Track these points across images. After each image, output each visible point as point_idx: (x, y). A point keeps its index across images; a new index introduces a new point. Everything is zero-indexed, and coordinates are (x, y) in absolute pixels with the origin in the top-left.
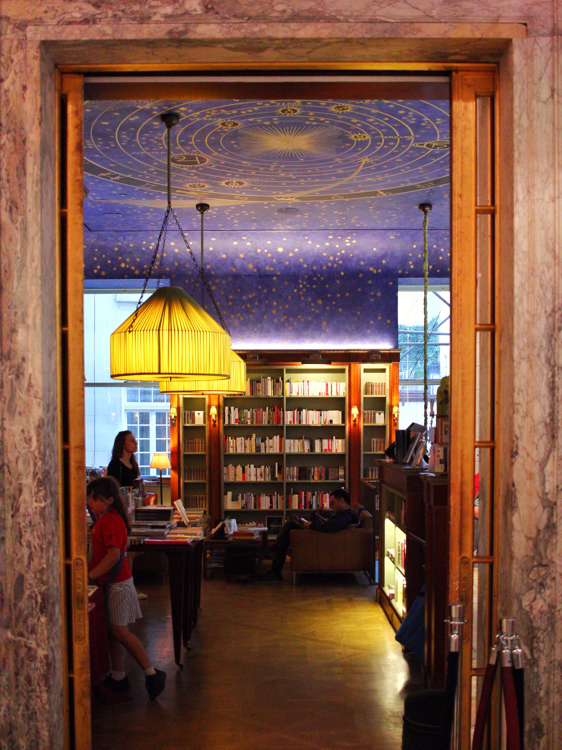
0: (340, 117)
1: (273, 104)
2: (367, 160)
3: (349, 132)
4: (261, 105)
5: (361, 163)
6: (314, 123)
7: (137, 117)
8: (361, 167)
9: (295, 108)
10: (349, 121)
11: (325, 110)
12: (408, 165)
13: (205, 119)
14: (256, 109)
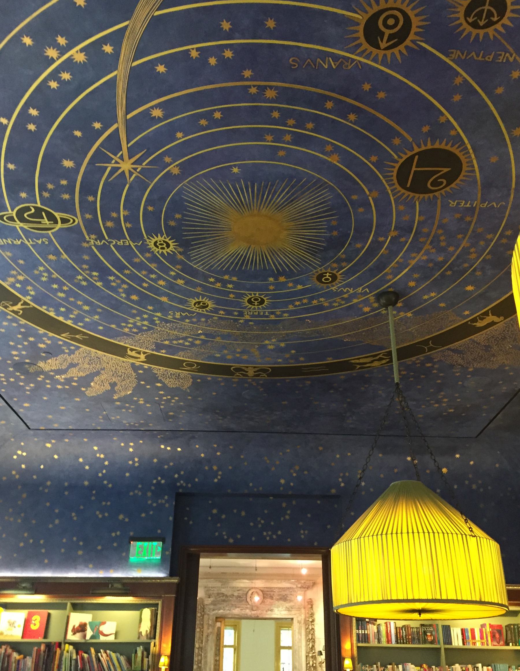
0: (198, 290)
1: (272, 313)
2: (126, 166)
4: (284, 312)
5: (131, 153)
6: (226, 277)
7: (426, 297)
8: (120, 125)
9: (250, 306)
11: (218, 302)
12: (39, 136)
13: (351, 291)
14: (291, 307)
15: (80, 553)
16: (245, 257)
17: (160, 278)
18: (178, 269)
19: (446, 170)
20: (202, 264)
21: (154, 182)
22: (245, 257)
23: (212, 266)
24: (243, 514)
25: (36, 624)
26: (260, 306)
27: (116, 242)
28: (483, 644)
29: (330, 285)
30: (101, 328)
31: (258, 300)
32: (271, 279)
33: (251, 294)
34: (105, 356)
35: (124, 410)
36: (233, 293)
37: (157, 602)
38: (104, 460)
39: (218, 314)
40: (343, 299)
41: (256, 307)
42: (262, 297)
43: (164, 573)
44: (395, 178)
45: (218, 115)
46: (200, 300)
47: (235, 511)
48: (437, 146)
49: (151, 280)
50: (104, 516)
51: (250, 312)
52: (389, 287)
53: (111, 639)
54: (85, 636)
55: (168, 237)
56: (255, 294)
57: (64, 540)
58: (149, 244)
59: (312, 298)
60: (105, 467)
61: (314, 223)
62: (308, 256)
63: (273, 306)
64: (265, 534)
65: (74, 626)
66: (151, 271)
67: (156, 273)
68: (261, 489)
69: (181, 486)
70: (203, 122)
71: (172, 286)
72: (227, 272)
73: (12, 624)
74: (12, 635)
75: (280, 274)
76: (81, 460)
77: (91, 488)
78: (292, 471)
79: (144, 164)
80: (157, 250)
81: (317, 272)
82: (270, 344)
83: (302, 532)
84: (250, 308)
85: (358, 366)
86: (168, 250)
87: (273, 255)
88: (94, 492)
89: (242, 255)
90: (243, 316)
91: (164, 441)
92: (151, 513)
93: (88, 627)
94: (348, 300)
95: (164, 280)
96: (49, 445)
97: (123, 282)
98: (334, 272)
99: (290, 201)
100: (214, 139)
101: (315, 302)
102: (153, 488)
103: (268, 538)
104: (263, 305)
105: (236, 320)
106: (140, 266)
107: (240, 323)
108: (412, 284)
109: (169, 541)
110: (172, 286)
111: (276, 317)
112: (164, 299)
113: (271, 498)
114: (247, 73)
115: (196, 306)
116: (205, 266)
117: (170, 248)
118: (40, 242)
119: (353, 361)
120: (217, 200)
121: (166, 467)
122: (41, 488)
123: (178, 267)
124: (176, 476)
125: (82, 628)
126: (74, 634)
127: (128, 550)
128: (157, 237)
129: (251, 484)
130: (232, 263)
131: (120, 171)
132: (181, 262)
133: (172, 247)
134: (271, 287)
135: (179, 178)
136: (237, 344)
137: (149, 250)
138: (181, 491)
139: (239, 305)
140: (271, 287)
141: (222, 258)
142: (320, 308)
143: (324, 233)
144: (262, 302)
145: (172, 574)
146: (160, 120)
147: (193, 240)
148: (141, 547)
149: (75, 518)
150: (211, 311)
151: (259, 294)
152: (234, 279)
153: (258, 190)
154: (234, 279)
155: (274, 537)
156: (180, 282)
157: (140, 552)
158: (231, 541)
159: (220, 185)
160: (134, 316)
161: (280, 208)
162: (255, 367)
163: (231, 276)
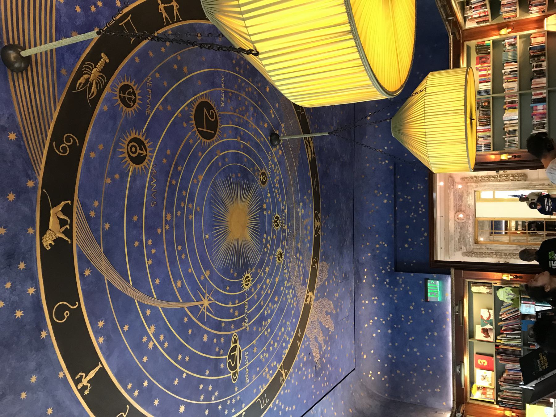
0: (271, 258)
1: (283, 211)
2: (206, 303)
3: (253, 270)
4: (283, 204)
6: (264, 241)
7: (273, 116)
8: (185, 306)
9: (280, 225)
10: (267, 265)
11: (278, 246)
12: (192, 355)
13: (270, 163)
14: (280, 200)
15: (436, 334)
16: (253, 229)
17: (265, 282)
18: (260, 271)
19: (205, 110)
20: (257, 256)
21: (214, 286)
22: (253, 229)
23: (258, 250)
24: (408, 227)
25: (483, 362)
26: (280, 219)
27: (246, 310)
28: (489, 70)
29: (267, 176)
30: (294, 320)
31: (276, 221)
32: (265, 213)
33: (273, 225)
34: (310, 318)
35: (342, 307)
36: (273, 236)
37: (467, 282)
38: (374, 320)
39: (284, 246)
40: (275, 168)
41: (280, 221)
42: (274, 218)
43: (448, 279)
44: (210, 141)
45: (180, 248)
46: (277, 257)
47: (406, 232)
48: (193, 117)
49: (266, 288)
50: (411, 319)
51: (283, 225)
52: (268, 139)
53: (492, 312)
54: (491, 329)
55: (243, 277)
56: (273, 223)
57: (428, 344)
58: (247, 289)
59: (275, 187)
60: (378, 319)
61: (234, 188)
62: (252, 190)
63: (279, 211)
64: (421, 212)
65: (484, 337)
66: (262, 288)
67: (262, 285)
68: (391, 215)
69: (390, 268)
70: (183, 256)
71: (270, 275)
72: (261, 241)
73: (484, 378)
74: (492, 378)
75: (262, 208)
76: (374, 335)
77: (392, 328)
78: (378, 195)
79: (205, 292)
80: (250, 284)
81: (260, 185)
82: (301, 212)
83: (419, 188)
84: (281, 225)
85: (313, 155)
86: (250, 277)
87: (251, 212)
88: (395, 326)
89: (252, 231)
90: (286, 230)
91: (360, 280)
92: (408, 288)
93: (484, 327)
94: (276, 165)
95: (266, 279)
96: (365, 356)
97: (268, 305)
98: (260, 174)
99: (223, 203)
100: (192, 250)
101: (277, 185)
102: (392, 287)
103: (424, 210)
104: (279, 217)
105: (288, 235)
106: (259, 295)
107: (289, 231)
108: (266, 125)
109: (427, 275)
110: (270, 275)
111: (286, 209)
112: (277, 279)
113: (397, 208)
114: (159, 231)
115: (280, 259)
116: (258, 254)
117: (249, 276)
118: (247, 357)
119: (310, 159)
120: (223, 247)
121: (378, 279)
122: (394, 361)
123: (259, 271)
124: (383, 272)
125: (485, 331)
126: (489, 336)
127: (434, 302)
128: (243, 284)
129: (388, 222)
130: (256, 237)
131: (209, 307)
132: (256, 269)
133: (248, 275)
134: (269, 212)
135: (212, 271)
136: (302, 233)
137: (250, 289)
138: (393, 269)
139: (279, 232)
140: (269, 212)
141: (254, 243)
142: (280, 182)
143: (239, 181)
144: (277, 218)
145: (449, 273)
146: (182, 282)
147: (244, 262)
148: (431, 294)
149: (413, 338)
150: (283, 250)
151: (273, 220)
152: (265, 236)
153: (218, 222)
154: (265, 236)
155: (422, 206)
156: (267, 270)
157: (435, 295)
158: (426, 234)
159: (215, 245)
160: (287, 299)
161: (226, 209)
162: (315, 222)
163: (263, 237)
